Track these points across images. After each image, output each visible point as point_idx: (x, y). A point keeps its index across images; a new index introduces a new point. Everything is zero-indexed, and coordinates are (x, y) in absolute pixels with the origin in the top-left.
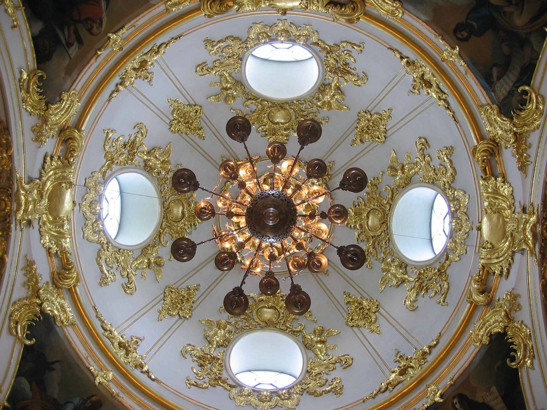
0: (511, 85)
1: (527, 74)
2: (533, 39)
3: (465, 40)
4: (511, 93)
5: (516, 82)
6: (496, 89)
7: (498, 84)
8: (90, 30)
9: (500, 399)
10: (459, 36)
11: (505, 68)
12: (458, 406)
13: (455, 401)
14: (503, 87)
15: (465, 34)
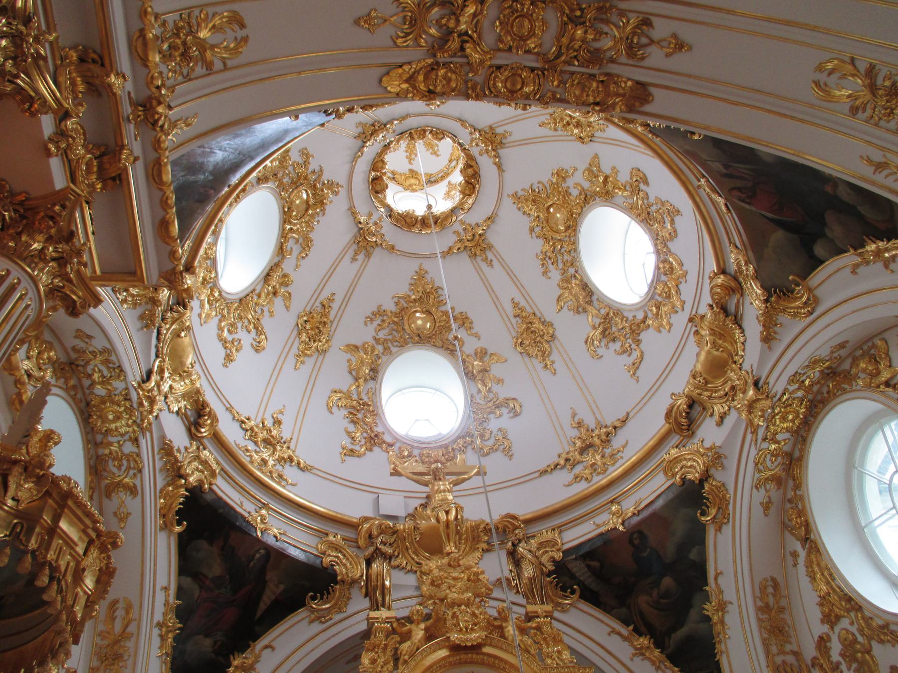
0: (582, 579)
1: (591, 597)
2: (624, 610)
3: (631, 541)
4: (572, 576)
5: (583, 584)
6: (579, 562)
7: (583, 565)
8: (739, 189)
9: (273, 597)
10: (635, 536)
11: (597, 574)
12: (258, 556)
13: (262, 551)
14: (579, 569)
15: (636, 542)
